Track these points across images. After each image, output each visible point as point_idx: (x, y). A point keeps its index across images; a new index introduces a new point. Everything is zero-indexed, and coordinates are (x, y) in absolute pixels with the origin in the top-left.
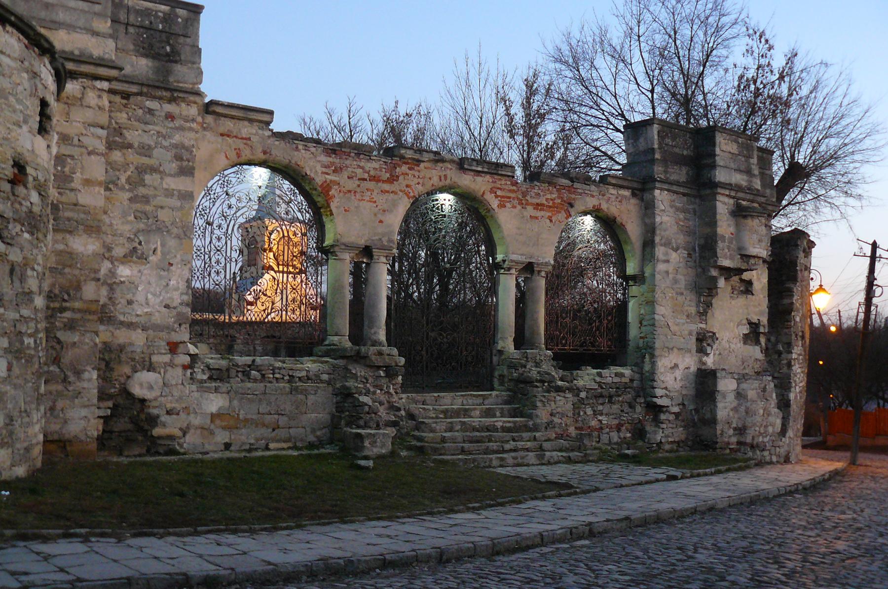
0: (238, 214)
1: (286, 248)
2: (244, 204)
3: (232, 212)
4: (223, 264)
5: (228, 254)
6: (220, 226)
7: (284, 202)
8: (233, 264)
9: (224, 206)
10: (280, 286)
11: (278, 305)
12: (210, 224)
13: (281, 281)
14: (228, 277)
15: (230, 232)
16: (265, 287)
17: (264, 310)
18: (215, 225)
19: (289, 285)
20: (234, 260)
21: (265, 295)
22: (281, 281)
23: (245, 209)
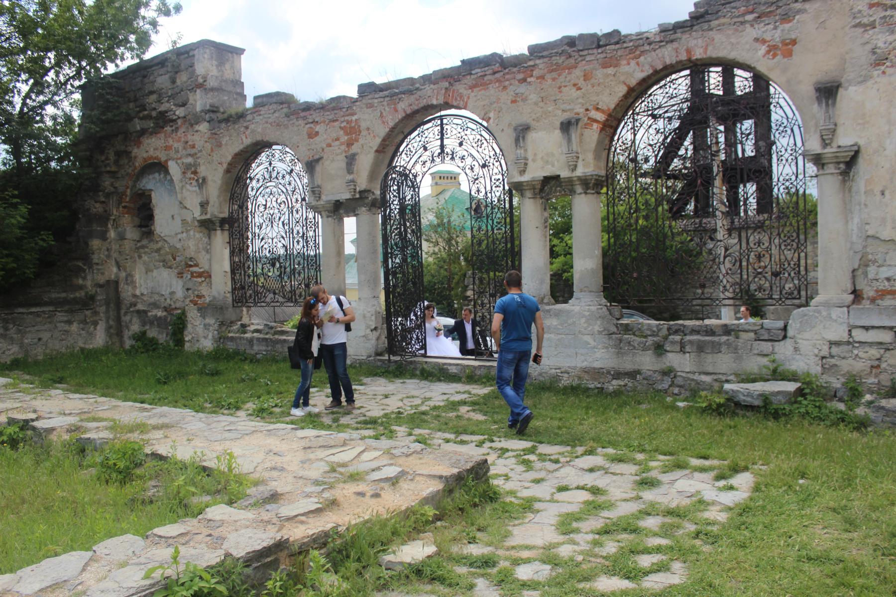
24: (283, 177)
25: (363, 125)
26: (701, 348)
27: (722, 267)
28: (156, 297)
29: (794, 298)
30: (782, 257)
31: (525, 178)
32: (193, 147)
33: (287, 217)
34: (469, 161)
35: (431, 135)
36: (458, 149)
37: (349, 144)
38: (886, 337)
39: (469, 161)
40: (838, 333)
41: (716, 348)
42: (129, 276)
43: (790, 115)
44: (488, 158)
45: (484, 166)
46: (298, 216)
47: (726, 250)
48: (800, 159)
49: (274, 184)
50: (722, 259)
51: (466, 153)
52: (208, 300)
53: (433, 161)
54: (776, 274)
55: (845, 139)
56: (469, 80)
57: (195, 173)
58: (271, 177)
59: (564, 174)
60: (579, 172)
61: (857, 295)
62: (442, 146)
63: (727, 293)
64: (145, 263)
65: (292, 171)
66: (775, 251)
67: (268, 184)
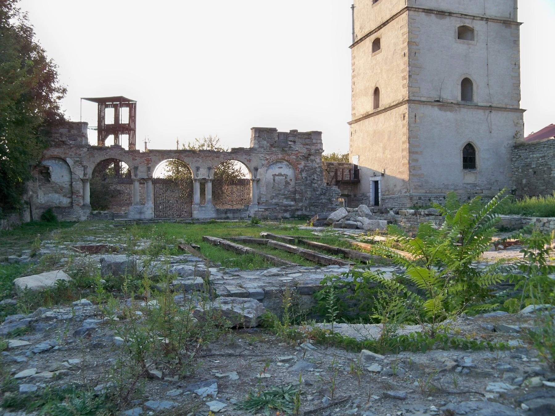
25: (153, 160)
26: (234, 213)
28: (51, 204)
31: (198, 178)
32: (80, 155)
37: (148, 164)
38: (263, 210)
40: (256, 209)
41: (237, 213)
42: (37, 196)
52: (82, 204)
55: (258, 177)
56: (184, 154)
57: (81, 164)
59: (207, 178)
60: (210, 178)
61: (259, 203)
64: (43, 191)
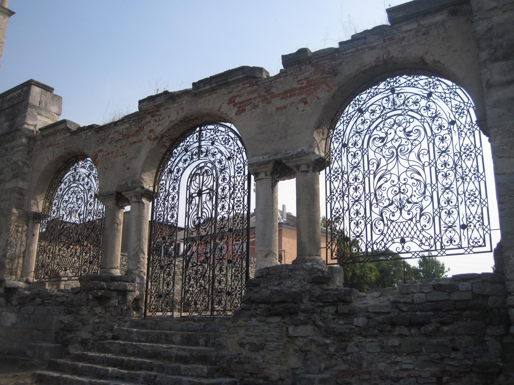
0: (372, 128)
1: (431, 145)
2: (378, 115)
3: (366, 127)
4: (361, 179)
5: (366, 169)
6: (355, 144)
7: (423, 97)
8: (372, 177)
9: (358, 122)
10: (429, 188)
11: (429, 210)
12: (344, 145)
13: (428, 181)
14: (367, 191)
15: (365, 146)
16: (409, 194)
17: (411, 219)
18: (350, 145)
19: (439, 186)
20: (372, 172)
21: (409, 203)
22: (428, 181)
23: (380, 120)
24: (83, 179)
27: (418, 224)
29: (480, 246)
30: (468, 212)
33: (83, 209)
34: (219, 156)
35: (191, 140)
36: (211, 147)
39: (219, 156)
43: (466, 100)
44: (233, 152)
45: (229, 159)
46: (90, 208)
47: (422, 210)
48: (477, 133)
49: (75, 185)
50: (418, 218)
51: (216, 150)
53: (192, 159)
54: (463, 227)
58: (74, 180)
62: (200, 147)
63: (423, 246)
65: (89, 174)
66: (462, 208)
67: (72, 186)
